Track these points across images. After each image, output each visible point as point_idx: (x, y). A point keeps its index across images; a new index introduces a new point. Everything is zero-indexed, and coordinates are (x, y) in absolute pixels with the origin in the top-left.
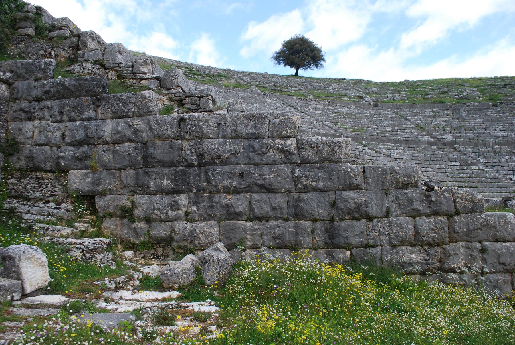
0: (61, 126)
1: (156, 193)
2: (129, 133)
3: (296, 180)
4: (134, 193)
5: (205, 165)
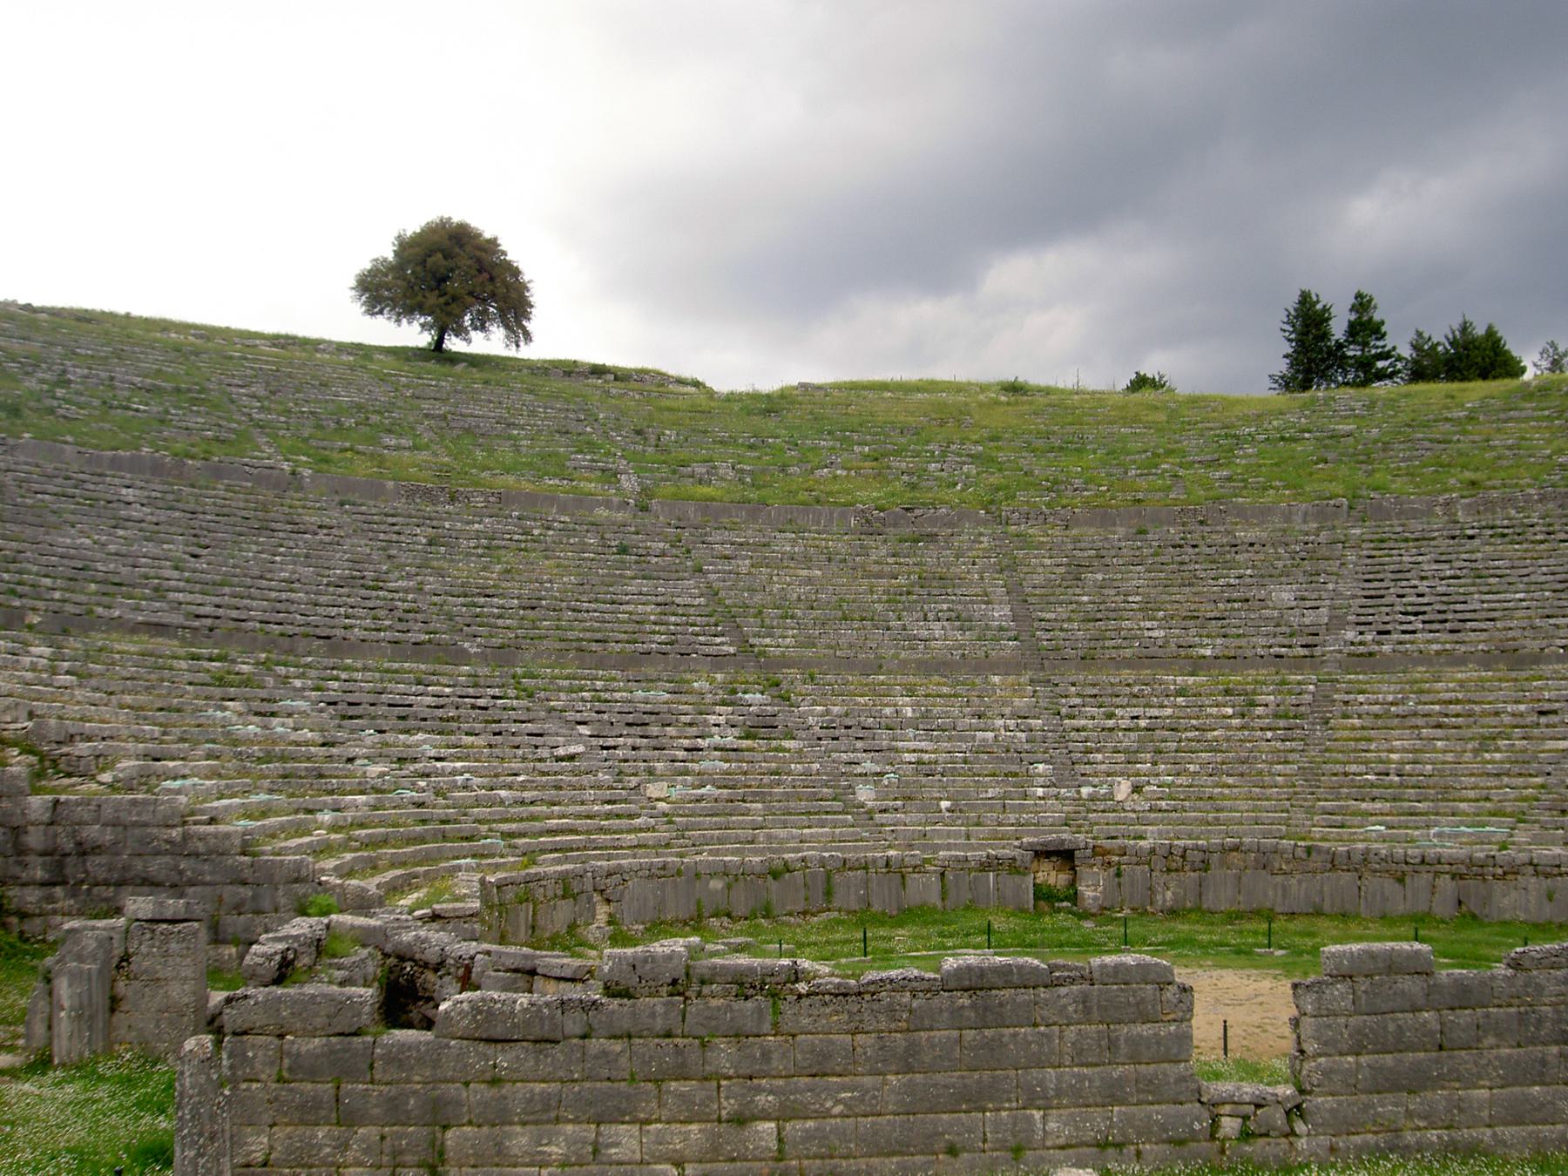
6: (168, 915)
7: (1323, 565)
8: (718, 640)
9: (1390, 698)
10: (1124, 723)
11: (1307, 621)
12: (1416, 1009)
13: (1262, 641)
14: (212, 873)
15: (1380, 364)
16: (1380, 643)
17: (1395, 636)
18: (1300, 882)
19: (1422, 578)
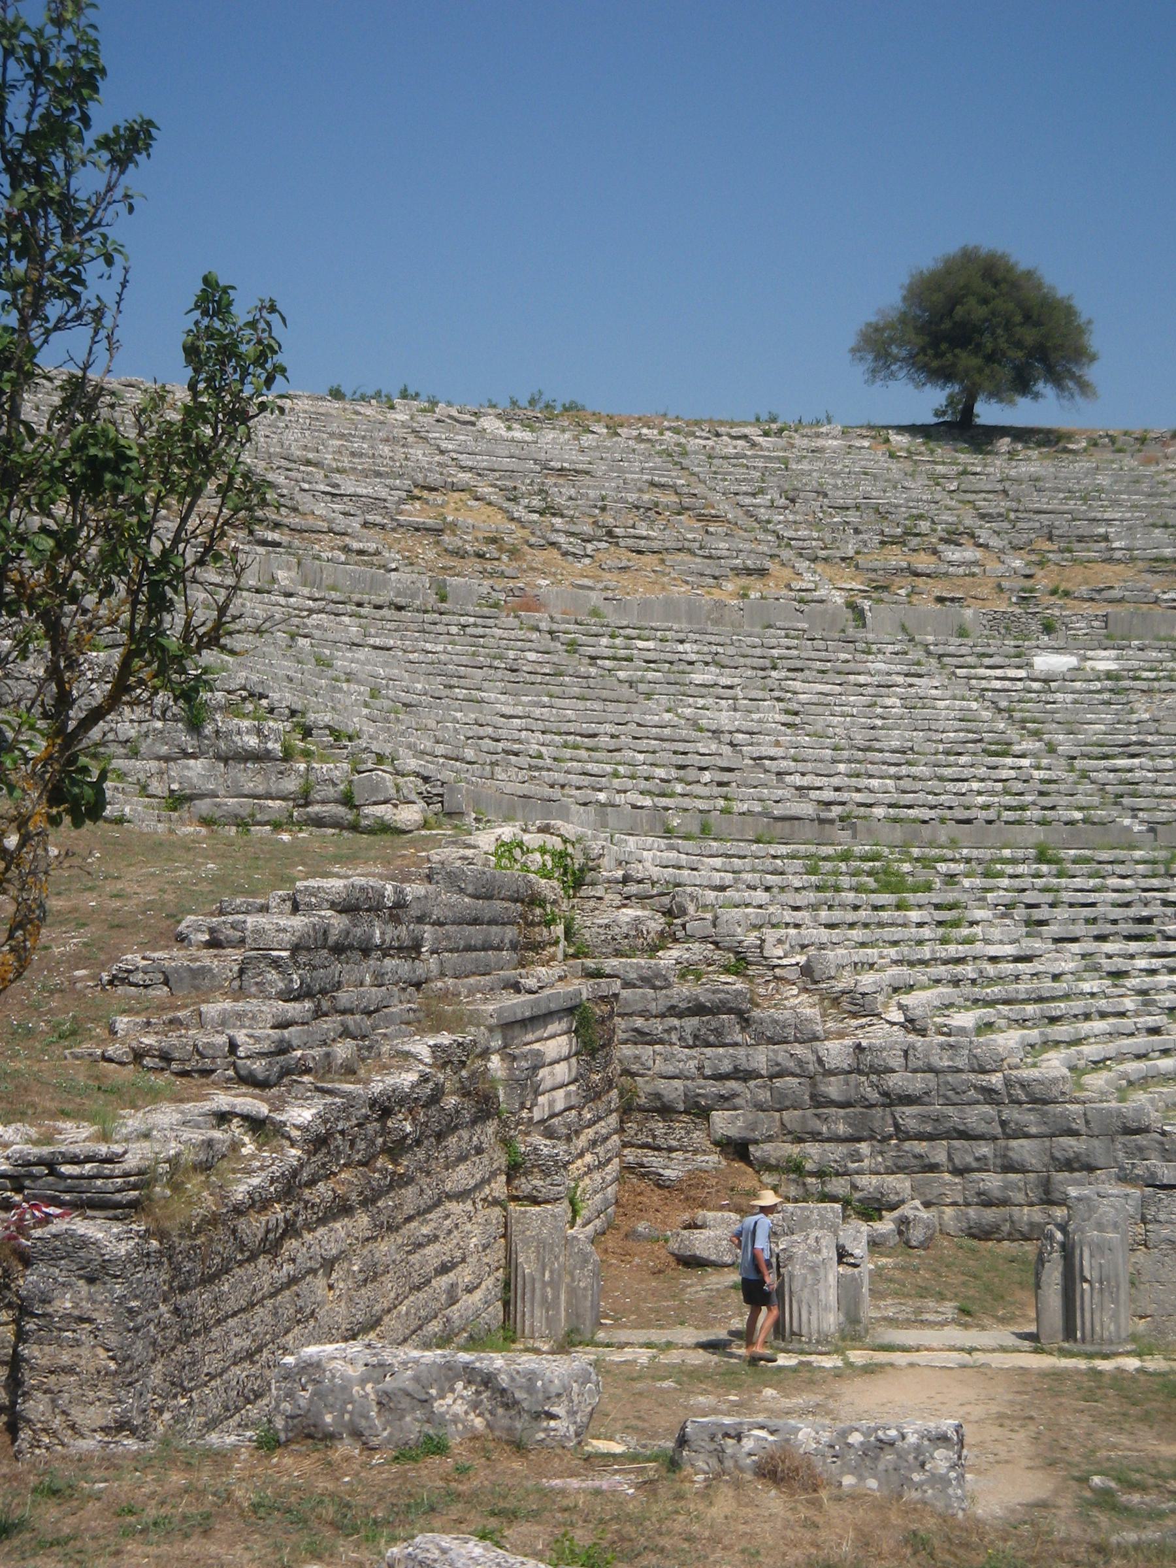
0: (694, 1052)
1: (829, 1140)
2: (791, 1064)
3: (1003, 1124)
4: (800, 1140)
5: (890, 1105)
14: (1038, 1124)
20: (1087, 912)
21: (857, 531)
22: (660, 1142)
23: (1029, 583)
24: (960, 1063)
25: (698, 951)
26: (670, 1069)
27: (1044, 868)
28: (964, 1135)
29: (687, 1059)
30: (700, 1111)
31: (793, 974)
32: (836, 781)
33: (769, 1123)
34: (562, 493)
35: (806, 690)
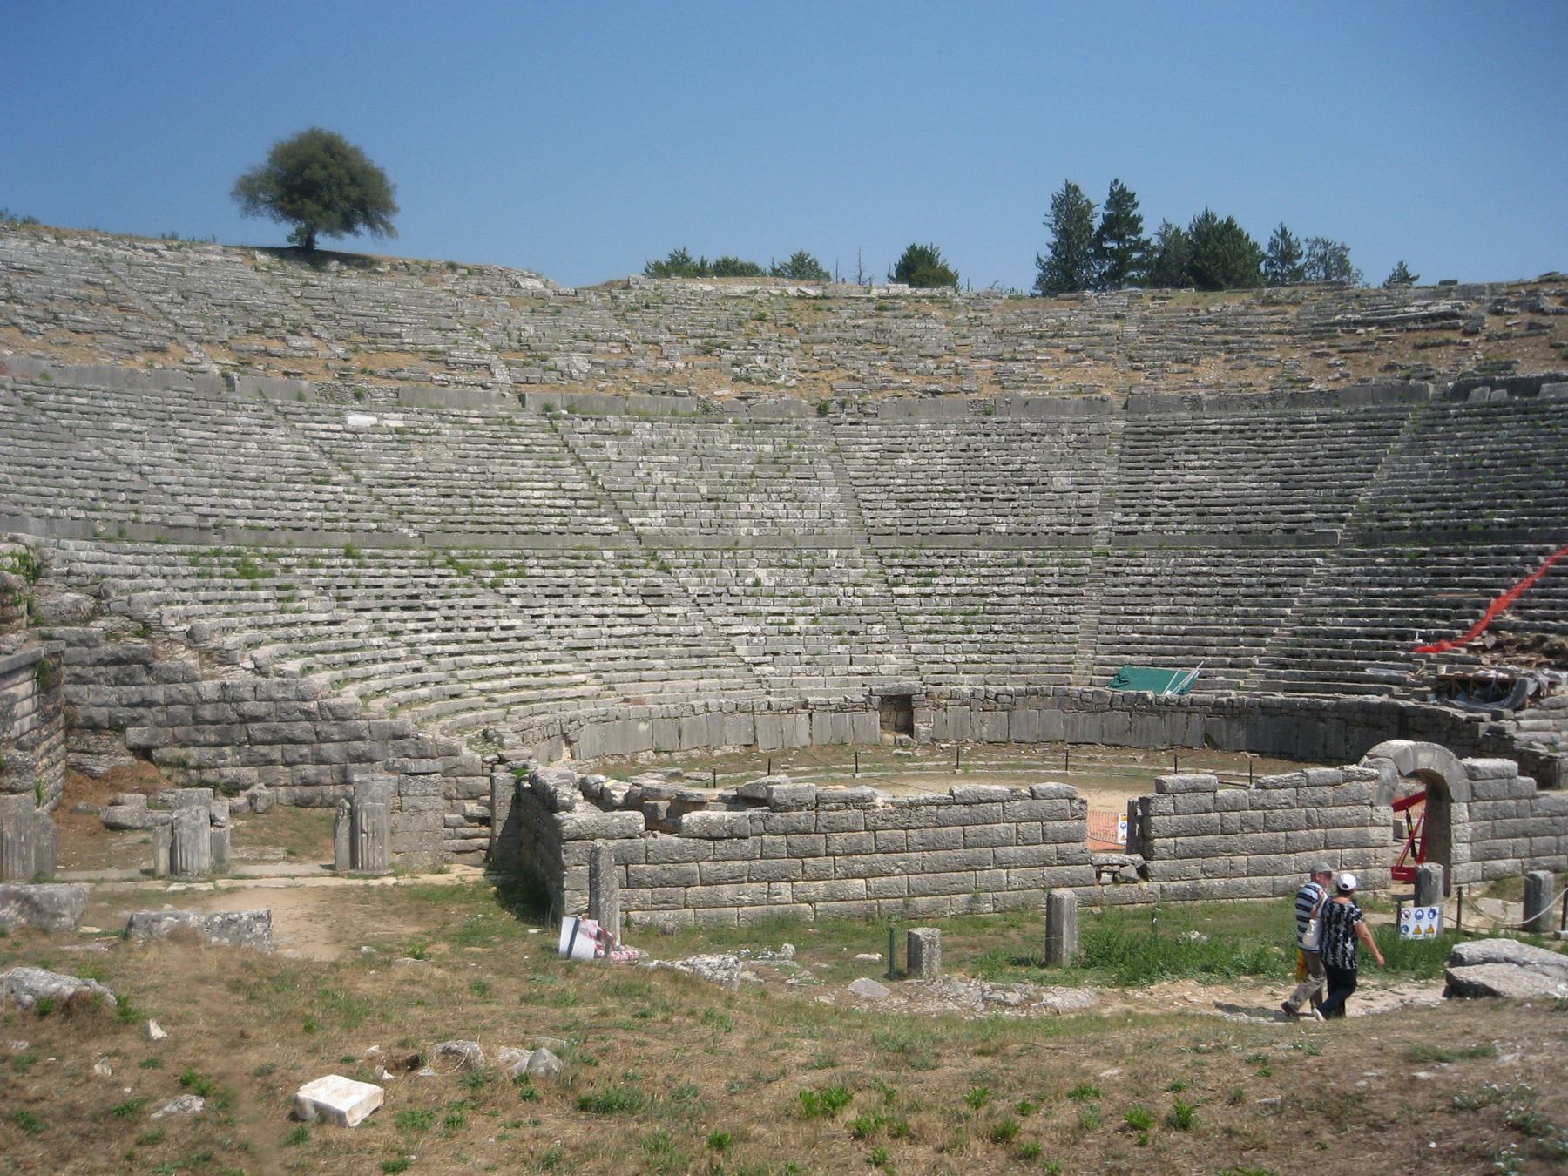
2: (180, 697)
3: (317, 733)
4: (185, 746)
6: (424, 770)
7: (1095, 454)
8: (603, 520)
9: (1151, 570)
10: (942, 589)
11: (1083, 503)
12: (1207, 811)
13: (1047, 519)
15: (1136, 255)
16: (1142, 523)
17: (1153, 518)
18: (1085, 719)
19: (1177, 467)
20: (376, 591)
21: (230, 323)
22: (93, 748)
23: (346, 365)
24: (290, 695)
25: (117, 622)
26: (99, 700)
27: (350, 561)
28: (292, 741)
29: (110, 694)
30: (118, 728)
31: (181, 638)
32: (212, 500)
33: (165, 735)
34: (22, 286)
35: (191, 435)
